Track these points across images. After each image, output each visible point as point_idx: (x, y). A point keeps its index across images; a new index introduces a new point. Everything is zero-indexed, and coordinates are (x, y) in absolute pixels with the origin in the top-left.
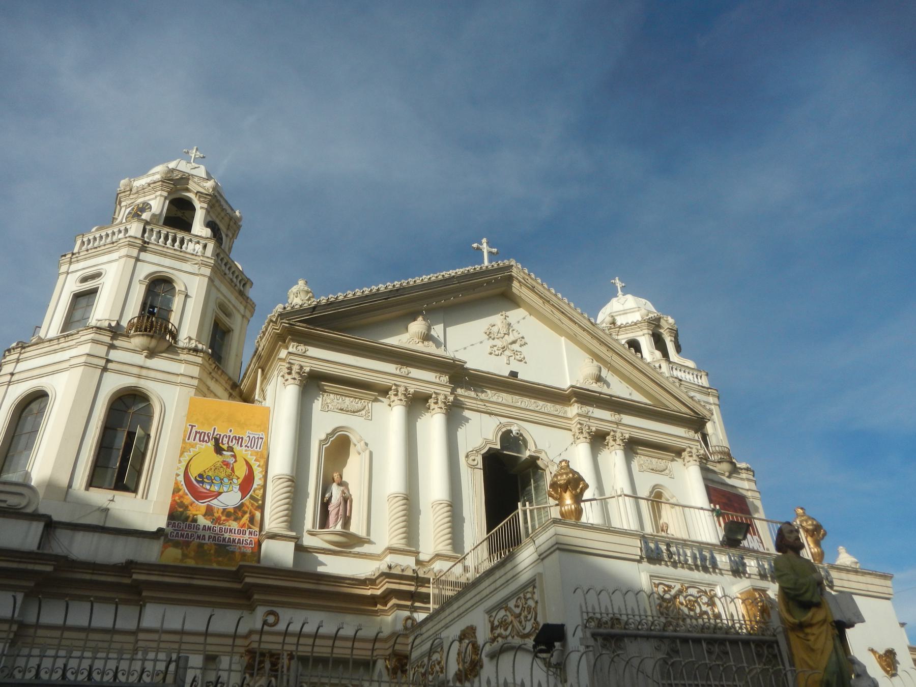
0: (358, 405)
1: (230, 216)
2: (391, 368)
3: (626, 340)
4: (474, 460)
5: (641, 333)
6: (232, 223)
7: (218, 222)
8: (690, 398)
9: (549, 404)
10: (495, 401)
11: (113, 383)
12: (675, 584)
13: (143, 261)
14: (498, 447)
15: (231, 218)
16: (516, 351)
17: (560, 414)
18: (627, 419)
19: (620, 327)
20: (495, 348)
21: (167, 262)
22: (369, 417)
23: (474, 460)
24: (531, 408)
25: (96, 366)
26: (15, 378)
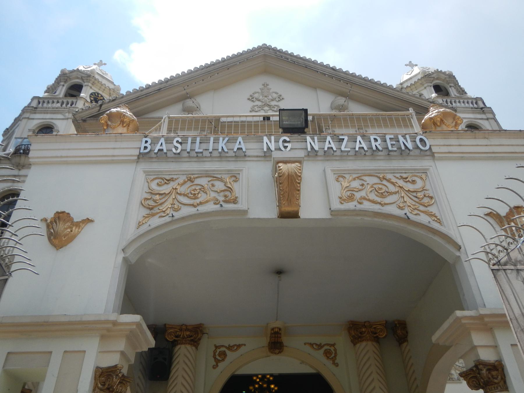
1: (109, 87)
5: (423, 88)
6: (112, 92)
7: (100, 92)
8: (431, 102)
12: (178, 176)
13: (33, 119)
15: (110, 89)
16: (275, 105)
20: (256, 107)
21: (48, 116)
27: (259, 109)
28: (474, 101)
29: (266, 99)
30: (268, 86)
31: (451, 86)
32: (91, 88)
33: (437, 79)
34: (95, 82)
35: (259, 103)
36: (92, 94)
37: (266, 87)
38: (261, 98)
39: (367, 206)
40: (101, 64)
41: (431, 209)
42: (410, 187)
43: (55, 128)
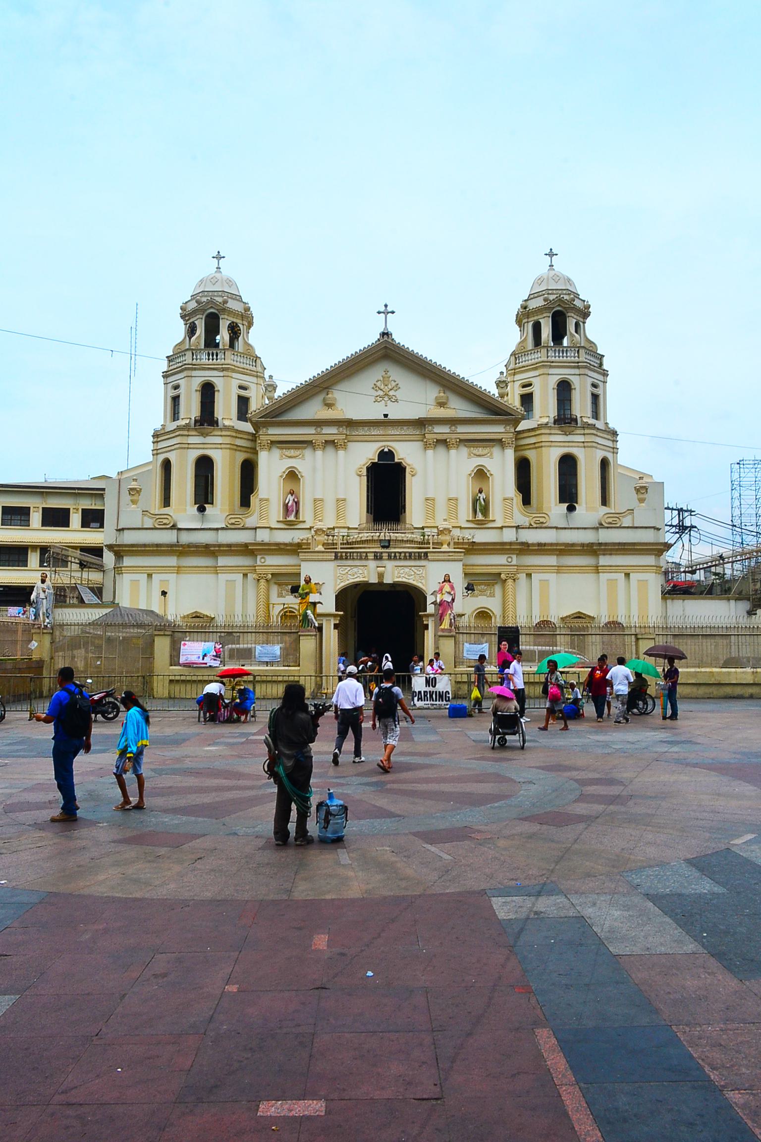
0: (297, 452)
2: (312, 430)
3: (532, 322)
4: (360, 472)
7: (235, 320)
9: (411, 427)
10: (376, 434)
11: (194, 454)
14: (376, 461)
17: (417, 433)
18: (461, 429)
19: (528, 313)
20: (378, 398)
22: (303, 458)
23: (360, 472)
24: (398, 433)
25: (185, 448)
26: (159, 451)
27: (381, 399)
28: (577, 349)
29: (386, 387)
30: (388, 373)
31: (569, 317)
32: (227, 319)
33: (559, 305)
34: (230, 312)
35: (381, 393)
36: (229, 327)
37: (386, 374)
38: (382, 387)
39: (404, 580)
40: (219, 257)
41: (422, 581)
42: (418, 573)
43: (216, 389)
